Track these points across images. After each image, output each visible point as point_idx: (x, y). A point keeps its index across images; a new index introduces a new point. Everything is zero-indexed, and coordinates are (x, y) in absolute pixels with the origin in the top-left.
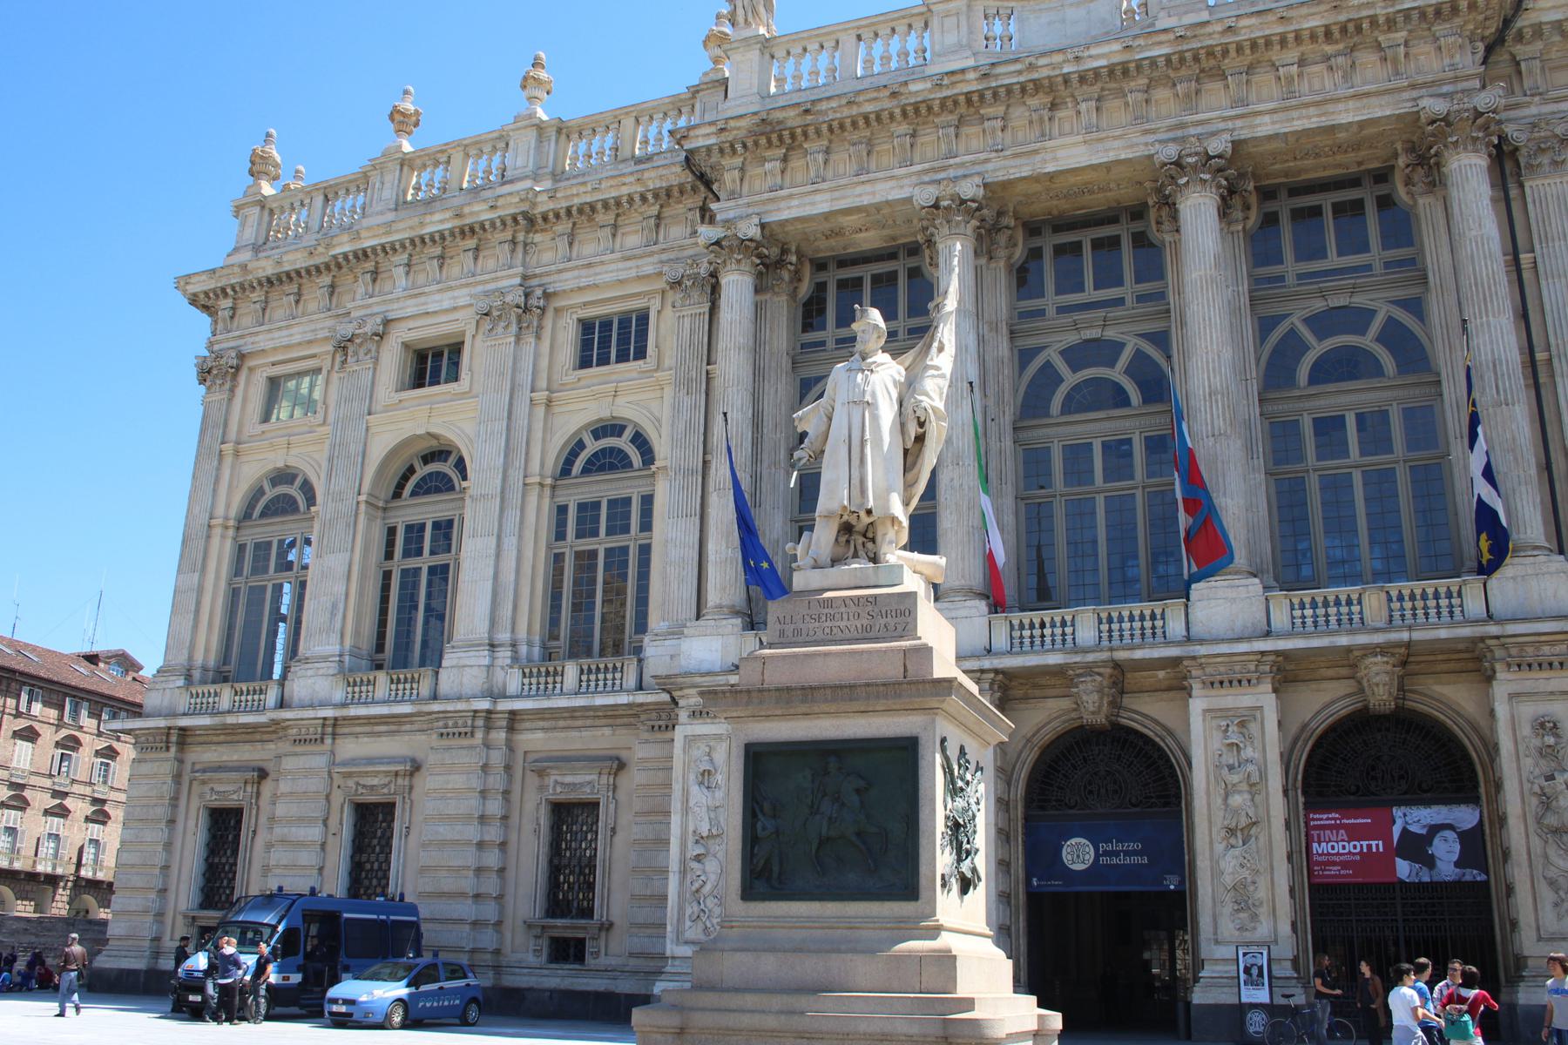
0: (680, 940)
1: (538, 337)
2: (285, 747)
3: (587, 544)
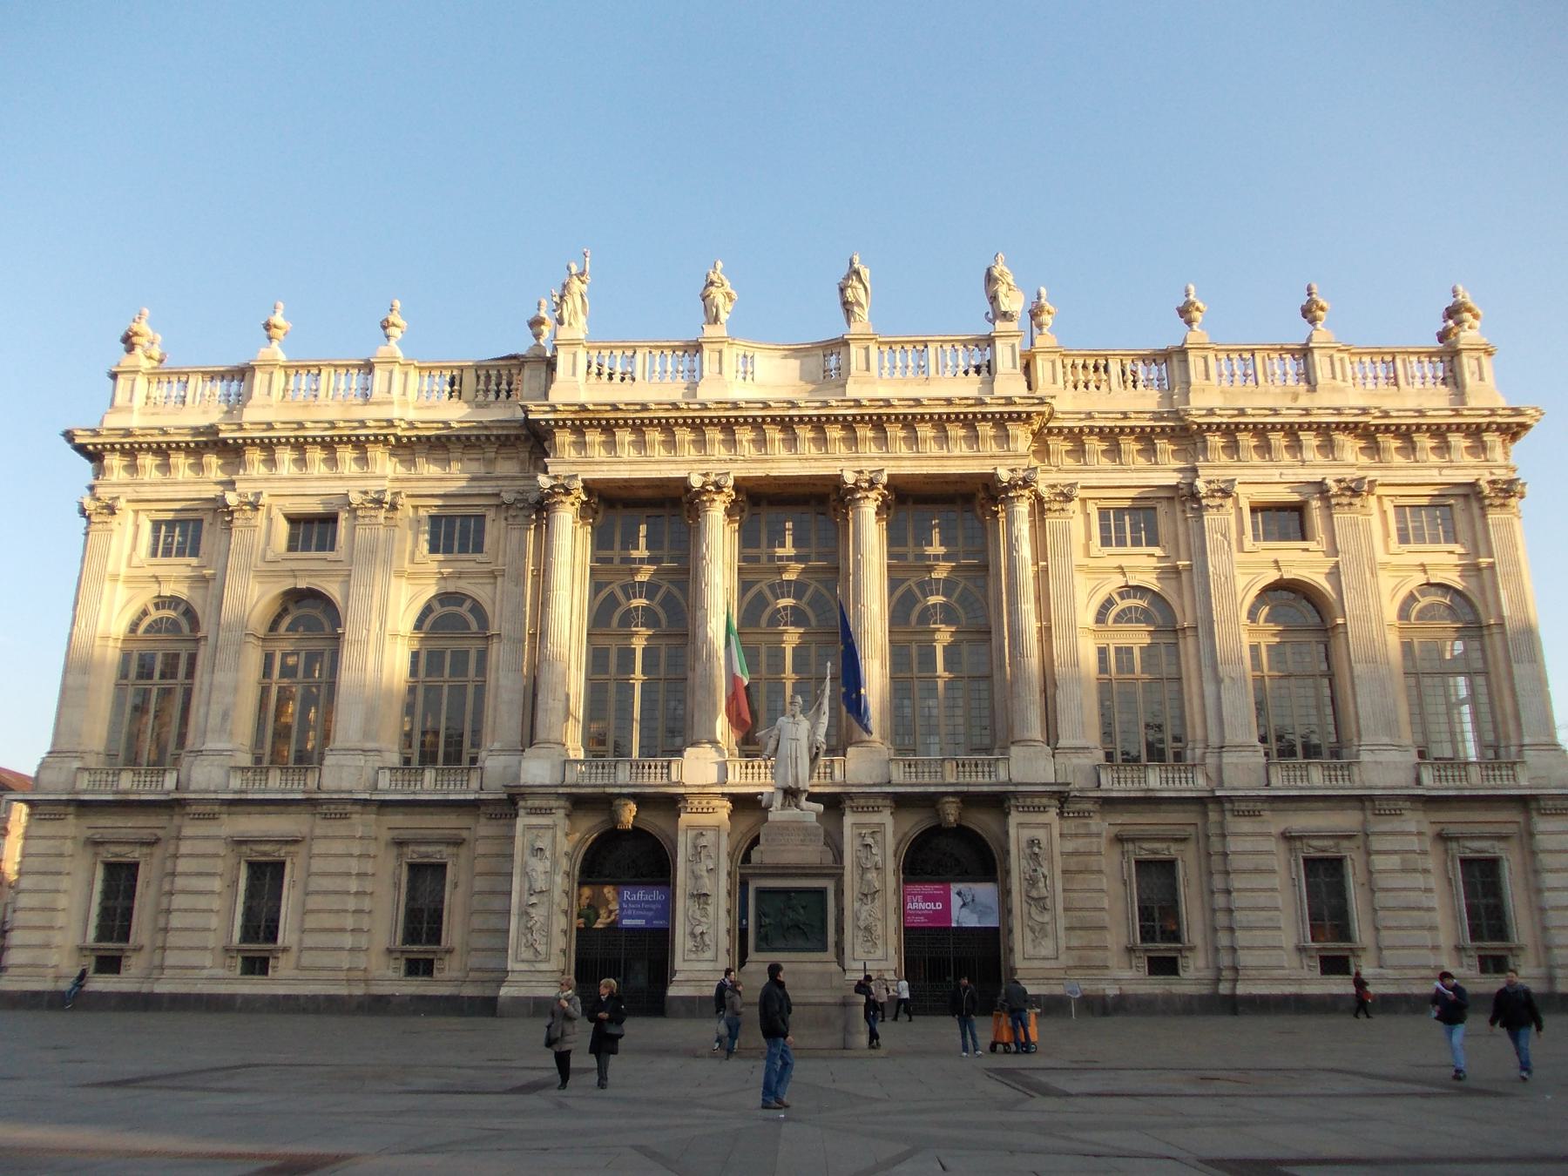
0: (517, 960)
2: (186, 821)
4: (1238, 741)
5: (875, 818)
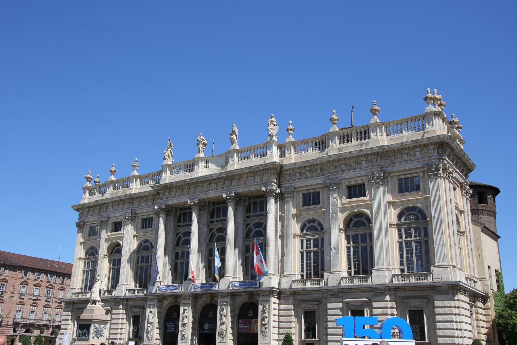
1: (134, 222)
3: (142, 265)
4: (335, 270)
5: (226, 300)
